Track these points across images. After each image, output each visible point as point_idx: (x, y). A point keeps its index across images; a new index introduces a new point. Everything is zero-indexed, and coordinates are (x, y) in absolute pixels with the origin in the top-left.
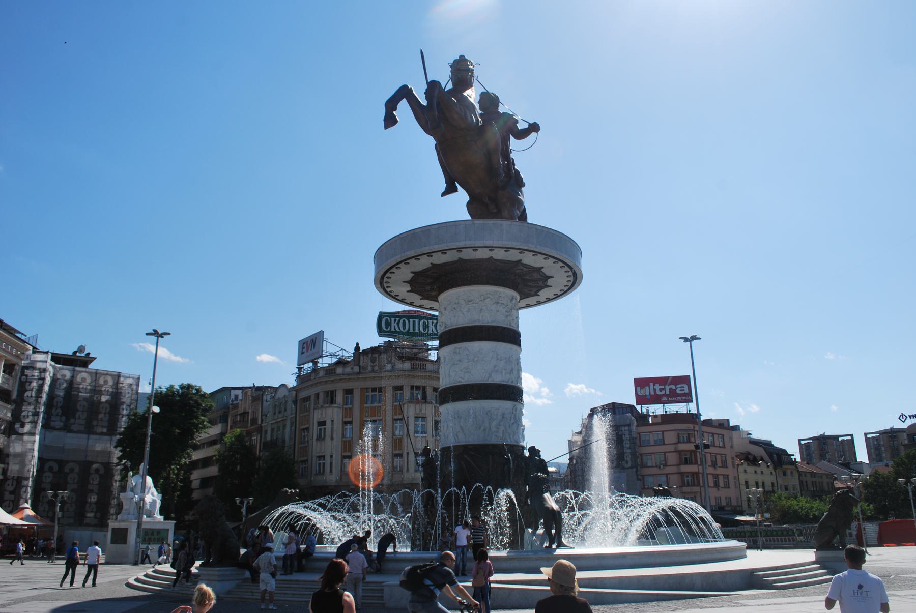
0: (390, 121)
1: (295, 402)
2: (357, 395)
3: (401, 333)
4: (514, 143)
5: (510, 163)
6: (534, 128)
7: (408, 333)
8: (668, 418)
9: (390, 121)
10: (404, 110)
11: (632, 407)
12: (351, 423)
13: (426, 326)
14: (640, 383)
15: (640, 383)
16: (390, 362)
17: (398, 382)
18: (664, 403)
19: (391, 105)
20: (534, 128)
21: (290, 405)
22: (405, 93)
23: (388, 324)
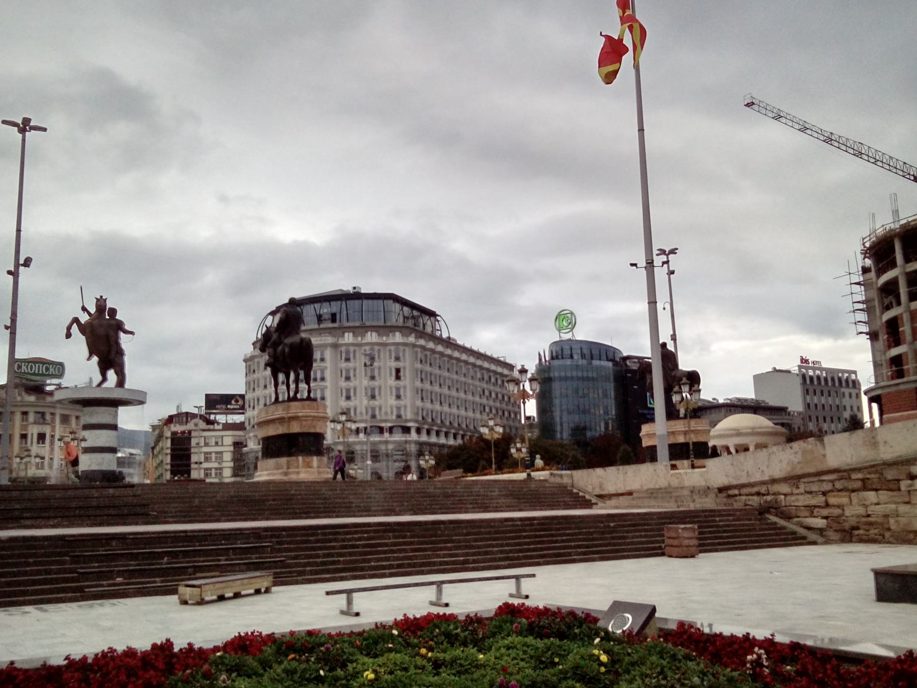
0: (68, 335)
3: (29, 373)
4: (122, 335)
5: (118, 344)
6: (132, 333)
7: (34, 374)
8: (228, 427)
9: (68, 335)
10: (75, 329)
11: (201, 417)
13: (47, 369)
14: (208, 397)
15: (208, 397)
16: (20, 395)
17: (25, 409)
18: (226, 414)
19: (69, 328)
20: (132, 333)
22: (76, 320)
23: (20, 367)
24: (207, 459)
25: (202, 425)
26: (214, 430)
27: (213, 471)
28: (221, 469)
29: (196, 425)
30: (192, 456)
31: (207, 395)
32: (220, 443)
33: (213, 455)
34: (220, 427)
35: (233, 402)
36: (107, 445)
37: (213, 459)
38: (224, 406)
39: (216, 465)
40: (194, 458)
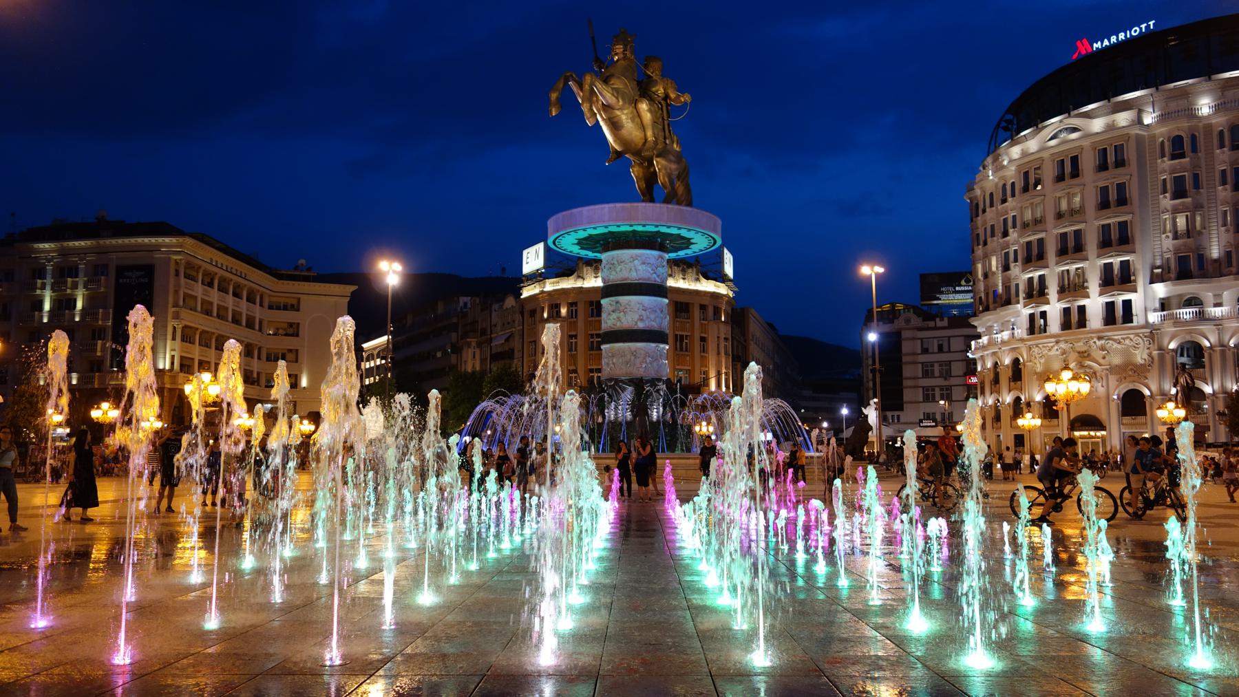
1: (522, 313)
2: (581, 308)
12: (576, 336)
21: (518, 317)
24: (927, 374)
25: (916, 321)
26: (936, 328)
27: (937, 392)
28: (949, 388)
29: (908, 321)
30: (904, 367)
31: (922, 276)
32: (945, 348)
33: (936, 365)
34: (945, 323)
35: (963, 282)
36: (641, 325)
37: (937, 373)
38: (951, 289)
39: (941, 382)
40: (907, 371)
